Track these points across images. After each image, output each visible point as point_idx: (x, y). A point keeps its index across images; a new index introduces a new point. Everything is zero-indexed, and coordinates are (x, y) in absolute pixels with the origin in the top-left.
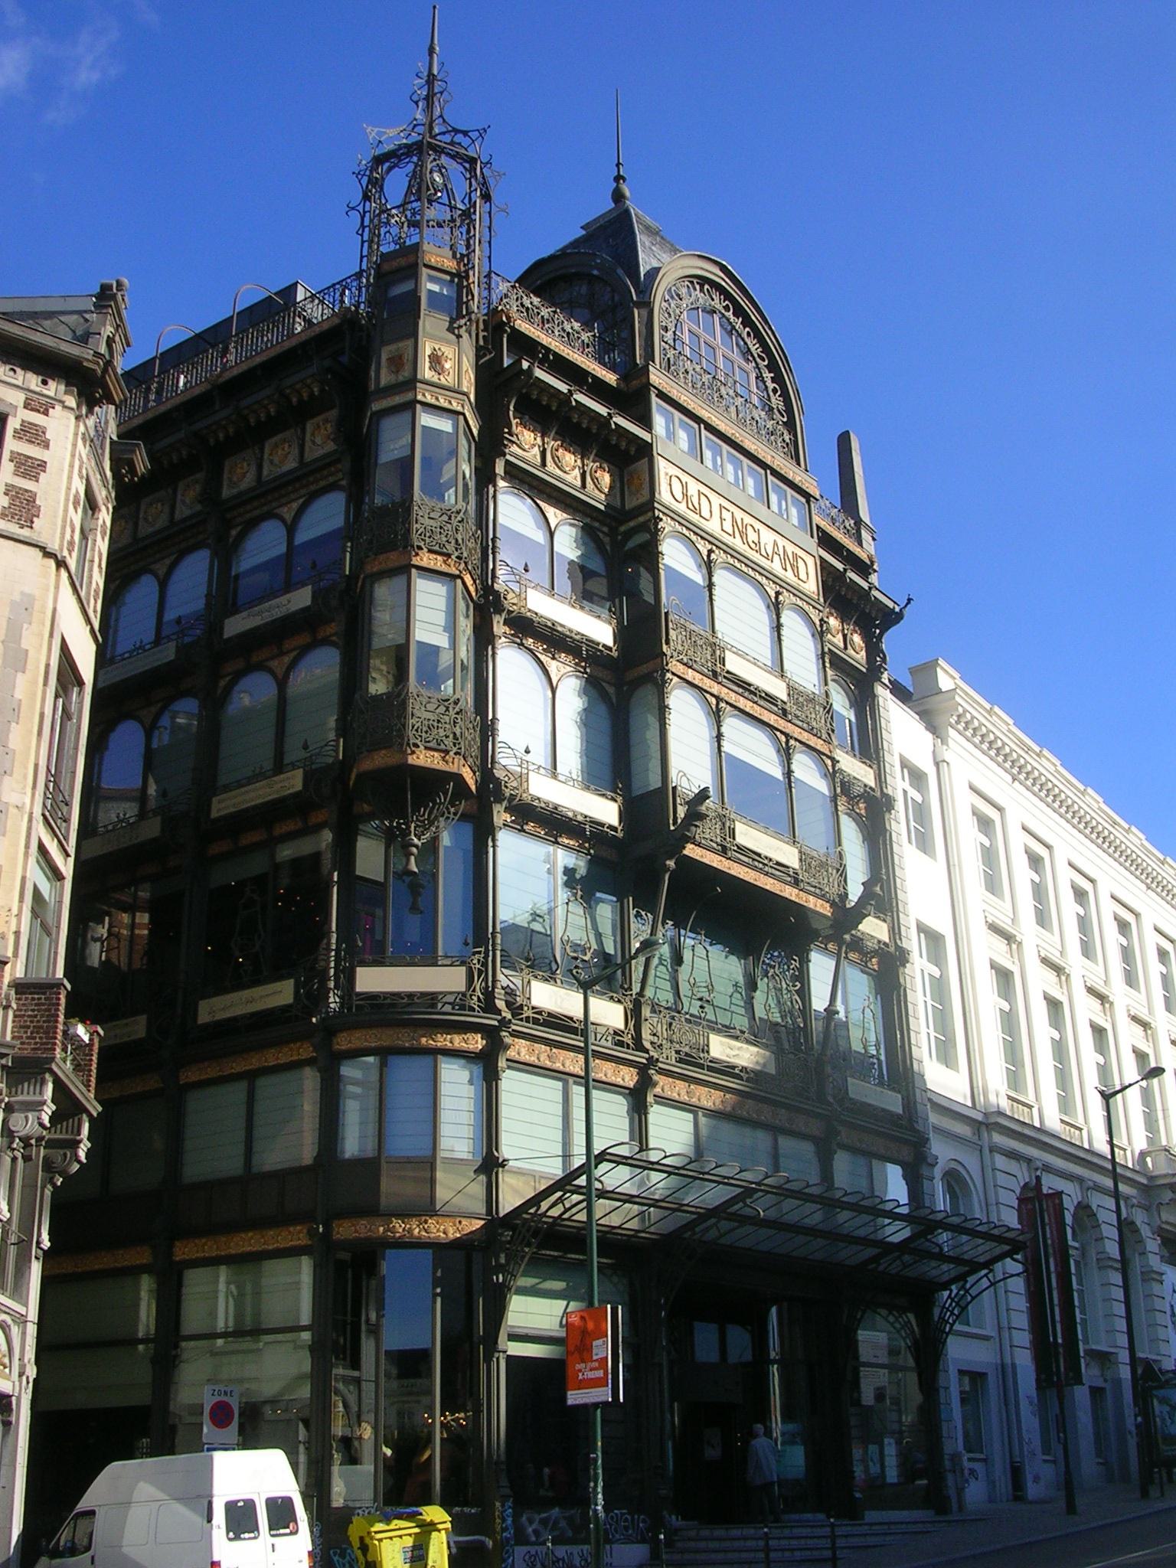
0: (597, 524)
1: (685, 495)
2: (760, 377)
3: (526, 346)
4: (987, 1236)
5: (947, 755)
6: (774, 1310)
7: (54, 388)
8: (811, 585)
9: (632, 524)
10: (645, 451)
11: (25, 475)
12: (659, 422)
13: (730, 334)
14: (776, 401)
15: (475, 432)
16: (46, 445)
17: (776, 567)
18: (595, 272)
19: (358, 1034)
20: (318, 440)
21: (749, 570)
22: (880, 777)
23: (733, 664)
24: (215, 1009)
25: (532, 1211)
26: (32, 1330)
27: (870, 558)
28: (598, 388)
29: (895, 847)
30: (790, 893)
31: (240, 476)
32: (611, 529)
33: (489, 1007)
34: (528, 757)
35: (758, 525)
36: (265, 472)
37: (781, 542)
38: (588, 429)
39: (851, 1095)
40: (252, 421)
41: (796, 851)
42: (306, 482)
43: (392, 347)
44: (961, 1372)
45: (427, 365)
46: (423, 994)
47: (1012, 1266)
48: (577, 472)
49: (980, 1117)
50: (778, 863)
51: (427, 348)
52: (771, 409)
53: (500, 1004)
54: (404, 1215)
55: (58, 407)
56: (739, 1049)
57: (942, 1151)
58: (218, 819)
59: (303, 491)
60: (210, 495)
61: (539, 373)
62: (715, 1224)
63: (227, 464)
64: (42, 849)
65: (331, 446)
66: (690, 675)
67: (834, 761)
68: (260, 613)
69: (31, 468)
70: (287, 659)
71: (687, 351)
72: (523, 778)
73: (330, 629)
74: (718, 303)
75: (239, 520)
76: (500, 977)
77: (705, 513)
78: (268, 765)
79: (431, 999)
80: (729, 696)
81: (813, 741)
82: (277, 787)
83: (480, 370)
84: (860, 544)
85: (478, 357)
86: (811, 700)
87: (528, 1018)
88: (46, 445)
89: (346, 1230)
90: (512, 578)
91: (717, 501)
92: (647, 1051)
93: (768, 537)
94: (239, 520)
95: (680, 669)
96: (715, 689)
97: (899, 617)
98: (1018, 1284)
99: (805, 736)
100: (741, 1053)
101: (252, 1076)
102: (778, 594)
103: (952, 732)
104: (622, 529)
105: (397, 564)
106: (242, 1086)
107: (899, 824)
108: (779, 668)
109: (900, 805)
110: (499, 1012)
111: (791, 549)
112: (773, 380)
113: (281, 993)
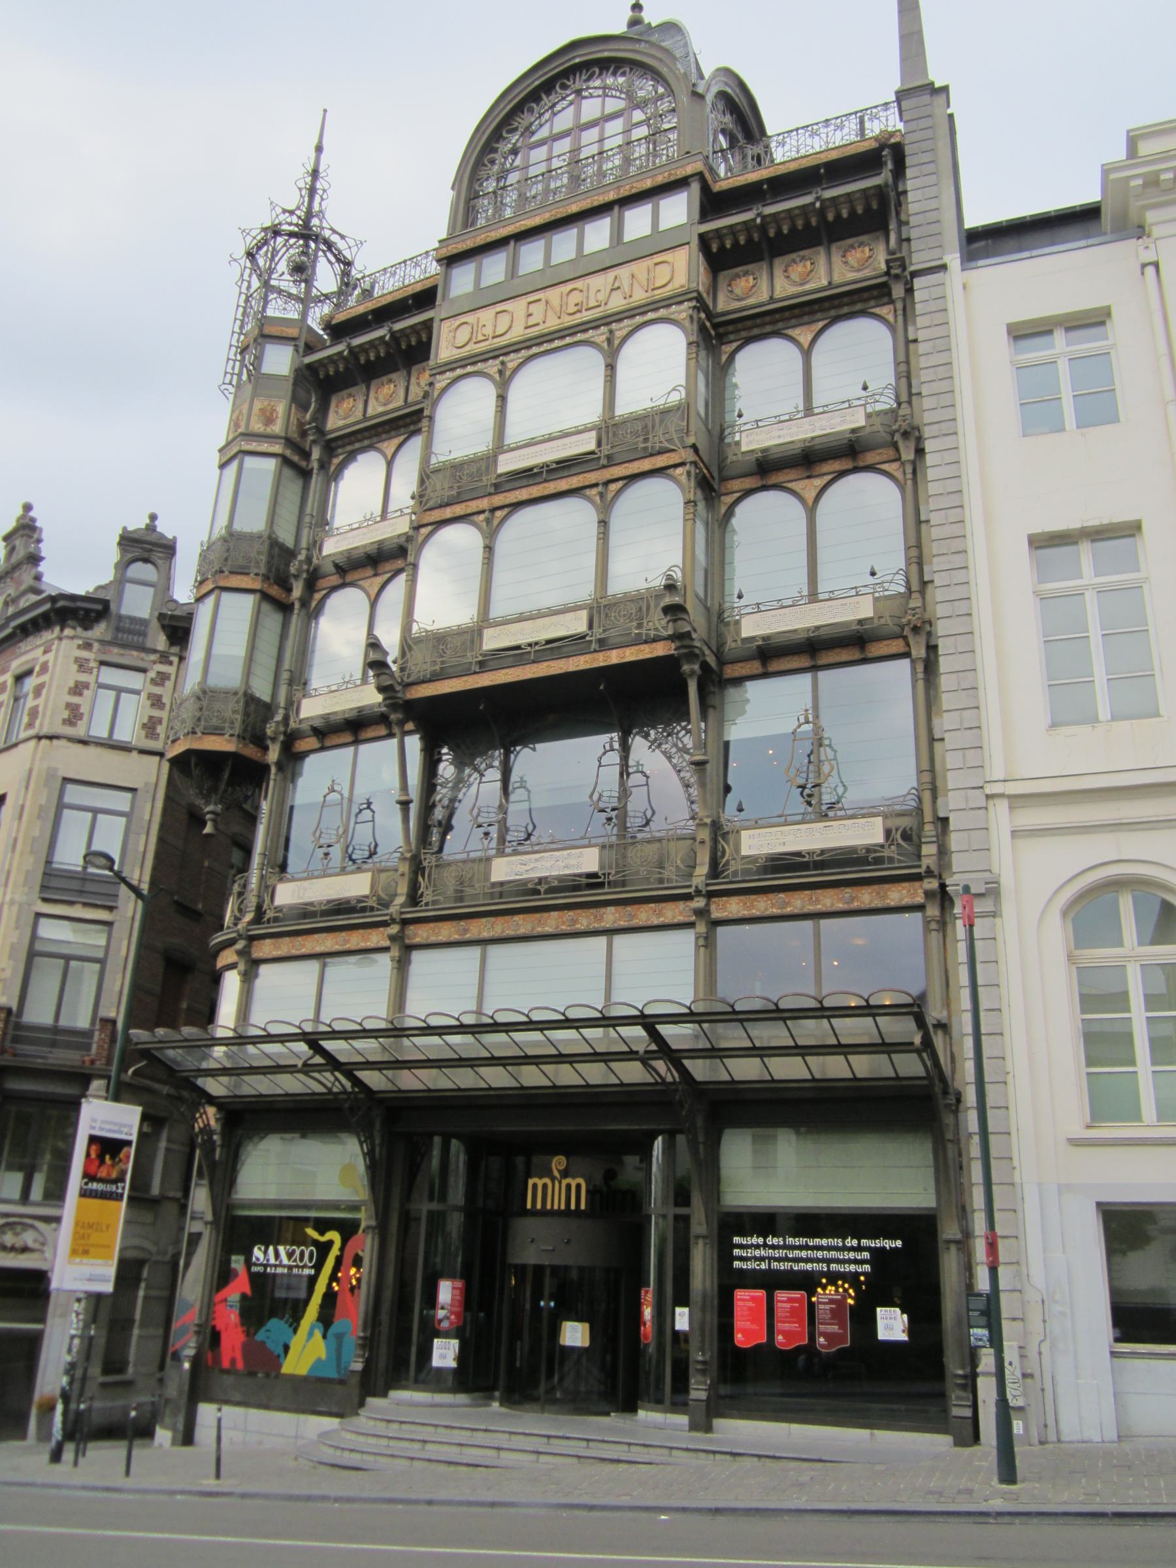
17: (617, 303)
37: (623, 272)
39: (745, 851)
44: (1099, 1205)
50: (549, 642)
55: (56, 642)
56: (537, 860)
66: (448, 513)
81: (646, 465)
87: (269, 921)
91: (518, 307)
95: (437, 515)
96: (484, 504)
100: (538, 864)
102: (611, 332)
103: (1150, 217)
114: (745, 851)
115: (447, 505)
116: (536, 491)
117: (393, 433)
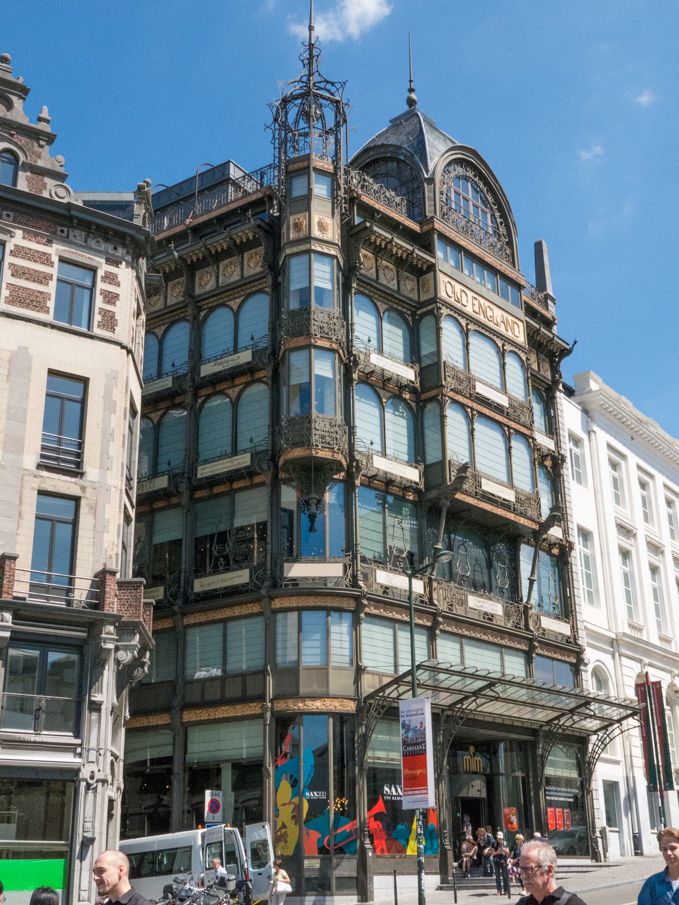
0: (404, 310)
1: (454, 292)
2: (493, 216)
3: (369, 212)
4: (619, 706)
5: (595, 428)
6: (502, 745)
7: (120, 252)
8: (521, 337)
9: (424, 310)
10: (432, 267)
11: (109, 302)
12: (439, 254)
13: (477, 192)
14: (502, 230)
15: (342, 264)
16: (118, 285)
17: (502, 329)
18: (402, 158)
19: (285, 599)
20: (252, 265)
21: (489, 333)
22: (558, 444)
23: (481, 389)
24: (201, 585)
25: (381, 694)
26: (122, 764)
27: (553, 317)
28: (407, 234)
29: (566, 484)
30: (511, 516)
31: (206, 283)
32: (412, 312)
33: (354, 583)
34: (373, 447)
35: (492, 306)
36: (220, 282)
37: (505, 315)
38: (402, 256)
39: (543, 626)
40: (213, 252)
41: (513, 492)
42: (245, 288)
43: (296, 216)
44: (604, 781)
45: (316, 228)
46: (320, 578)
47: (633, 722)
48: (395, 281)
49: (614, 636)
50: (504, 500)
51: (315, 219)
52: (499, 236)
53: (361, 583)
54: (314, 698)
57: (591, 656)
58: (201, 479)
59: (242, 293)
60: (189, 292)
61: (375, 229)
62: (474, 700)
63: (197, 273)
64: (125, 505)
65: (259, 269)
67: (534, 439)
68: (221, 364)
69: (111, 298)
70: (237, 389)
71: (453, 206)
72: (369, 458)
73: (261, 374)
74: (471, 174)
75: (205, 307)
76: (359, 568)
77: (464, 302)
78: (229, 449)
79: (325, 580)
80: (480, 409)
81: (522, 429)
82: (235, 463)
83: (342, 227)
84: (547, 309)
85: (342, 220)
86: (522, 406)
88: (118, 285)
89: (281, 706)
90: (362, 346)
92: (436, 606)
93: (498, 313)
94: (205, 307)
95: (451, 394)
96: (470, 403)
97: (569, 352)
98: (637, 732)
99: (517, 427)
101: (224, 621)
104: (418, 312)
105: (303, 344)
106: (221, 626)
107: (567, 471)
108: (504, 389)
109: (568, 460)
110: (360, 587)
111: (510, 318)
112: (501, 217)
113: (241, 577)
114: (543, 626)
115: (457, 393)
116: (486, 411)
117: (381, 299)
